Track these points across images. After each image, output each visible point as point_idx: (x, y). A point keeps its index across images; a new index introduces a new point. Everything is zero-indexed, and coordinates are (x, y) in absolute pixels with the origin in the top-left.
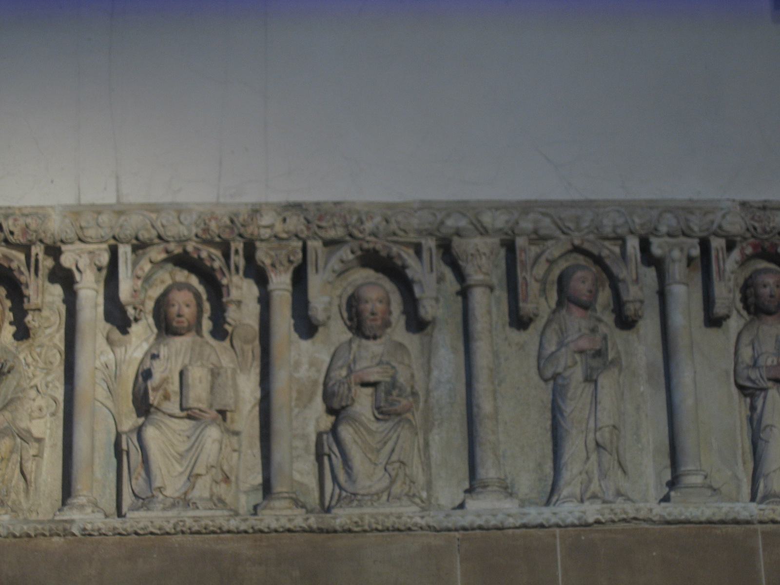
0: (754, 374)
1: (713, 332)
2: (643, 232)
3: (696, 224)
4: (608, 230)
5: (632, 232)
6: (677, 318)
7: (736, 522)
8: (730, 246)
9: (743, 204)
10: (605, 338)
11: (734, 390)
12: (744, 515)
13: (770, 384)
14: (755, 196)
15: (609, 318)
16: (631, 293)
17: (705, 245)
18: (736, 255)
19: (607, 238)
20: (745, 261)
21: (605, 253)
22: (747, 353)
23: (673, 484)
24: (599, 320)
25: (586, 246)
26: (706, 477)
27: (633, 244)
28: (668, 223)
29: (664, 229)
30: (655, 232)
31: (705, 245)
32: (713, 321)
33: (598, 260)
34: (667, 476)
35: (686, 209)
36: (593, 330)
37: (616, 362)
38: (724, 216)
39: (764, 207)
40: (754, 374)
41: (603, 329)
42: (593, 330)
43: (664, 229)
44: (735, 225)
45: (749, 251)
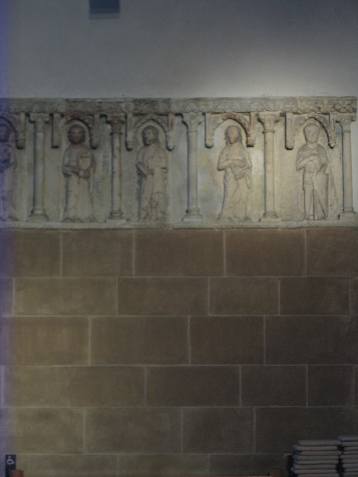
0: (67, 169)
1: (55, 151)
2: (26, 111)
3: (47, 108)
4: (13, 110)
5: (22, 111)
6: (39, 147)
7: (52, 229)
8: (63, 116)
9: (67, 100)
10: (9, 155)
11: (61, 174)
12: (55, 227)
13: (72, 174)
14: (73, 96)
15: (13, 145)
16: (21, 136)
17: (52, 115)
18: (64, 120)
19: (12, 113)
20: (68, 122)
21: (11, 120)
22: (67, 160)
23: (32, 212)
24: (9, 146)
25: (4, 116)
26: (44, 210)
27: (23, 116)
28: (36, 108)
29: (34, 110)
30: (31, 111)
31: (52, 115)
32: (55, 147)
33: (9, 122)
34: (31, 208)
35: (43, 102)
36: (6, 151)
37: (15, 165)
38: (58, 105)
39: (76, 101)
40: (67, 169)
41: (10, 150)
42: (6, 151)
43: (34, 110)
44: (63, 109)
45: (69, 118)
